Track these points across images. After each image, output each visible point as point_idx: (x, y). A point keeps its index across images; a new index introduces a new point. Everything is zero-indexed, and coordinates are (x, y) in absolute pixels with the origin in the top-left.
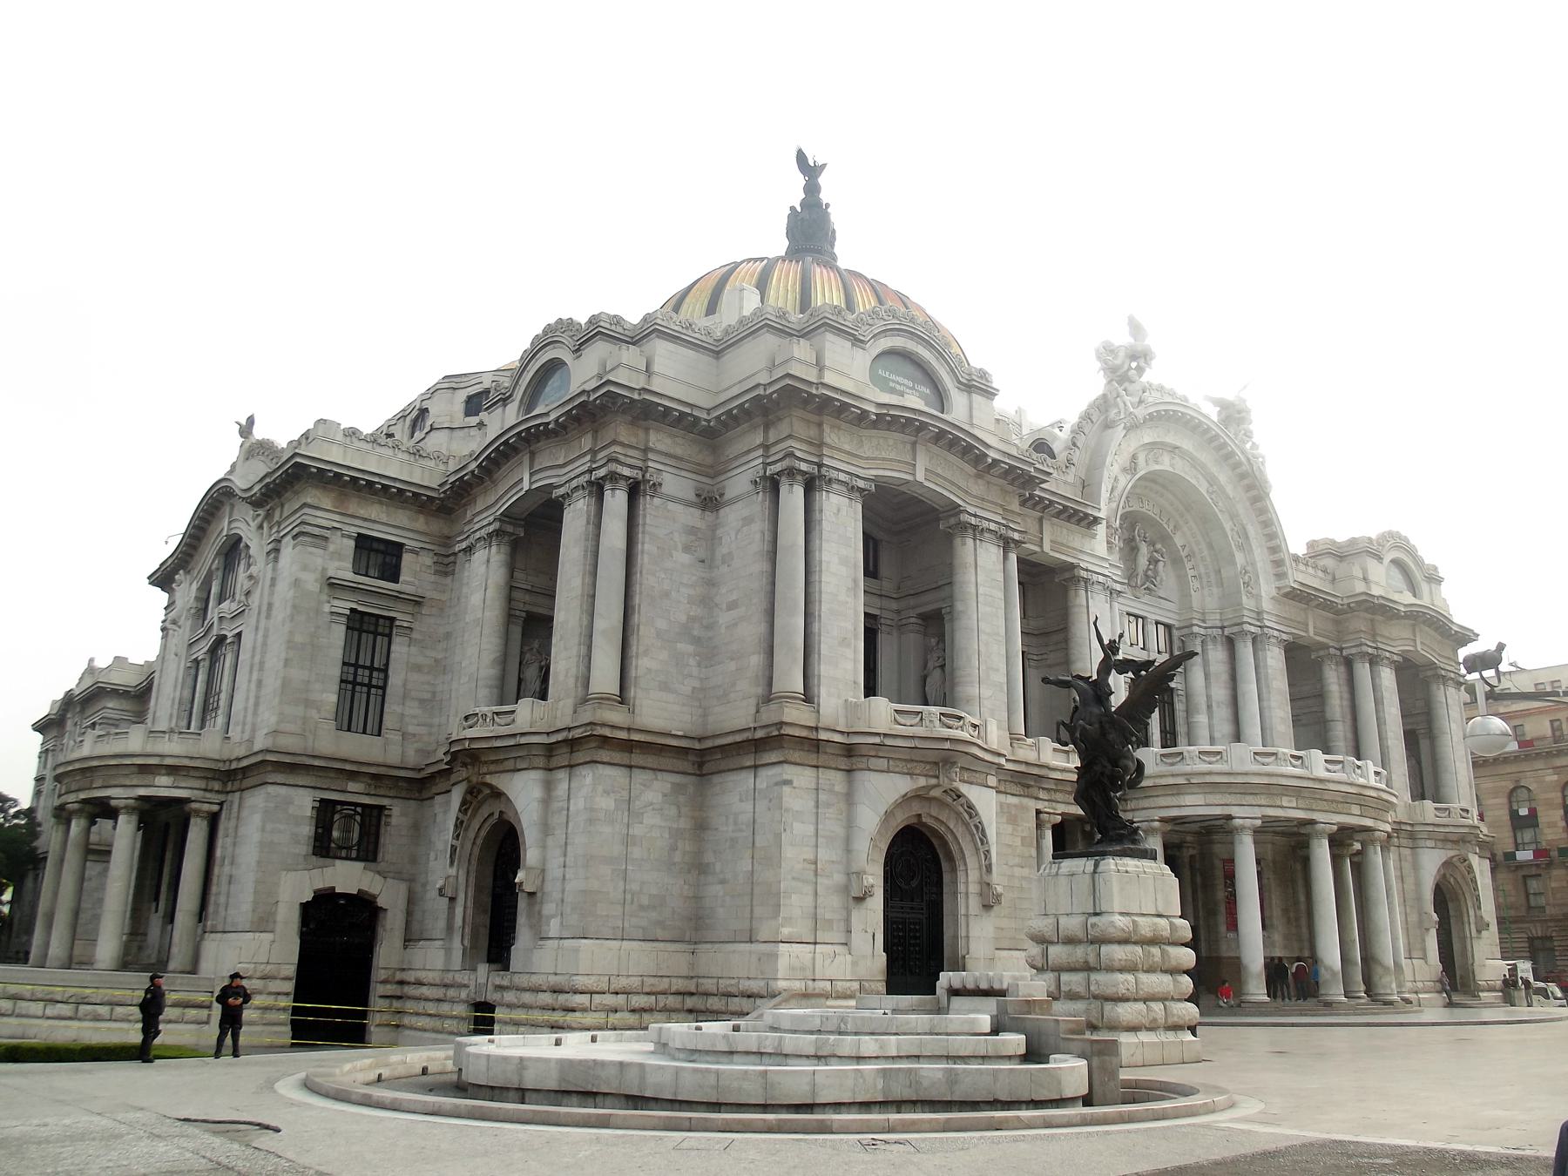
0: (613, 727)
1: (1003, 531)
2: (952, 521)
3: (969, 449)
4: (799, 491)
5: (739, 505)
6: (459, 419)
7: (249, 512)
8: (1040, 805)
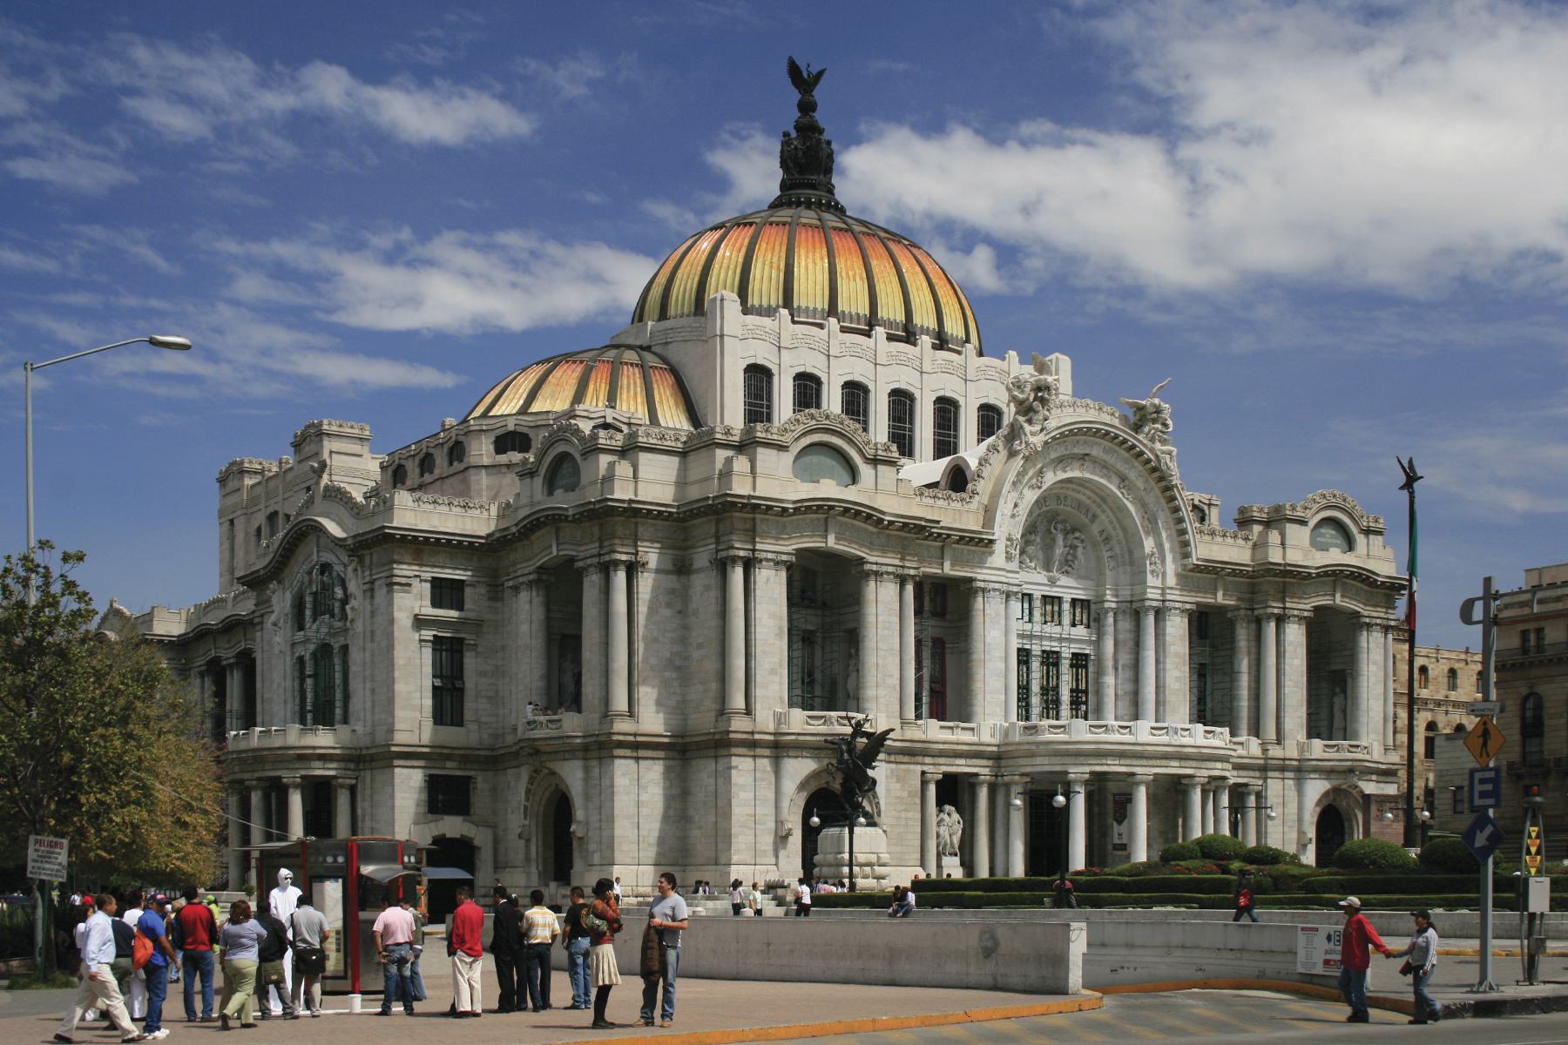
1: (900, 571)
5: (702, 575)
8: (926, 768)
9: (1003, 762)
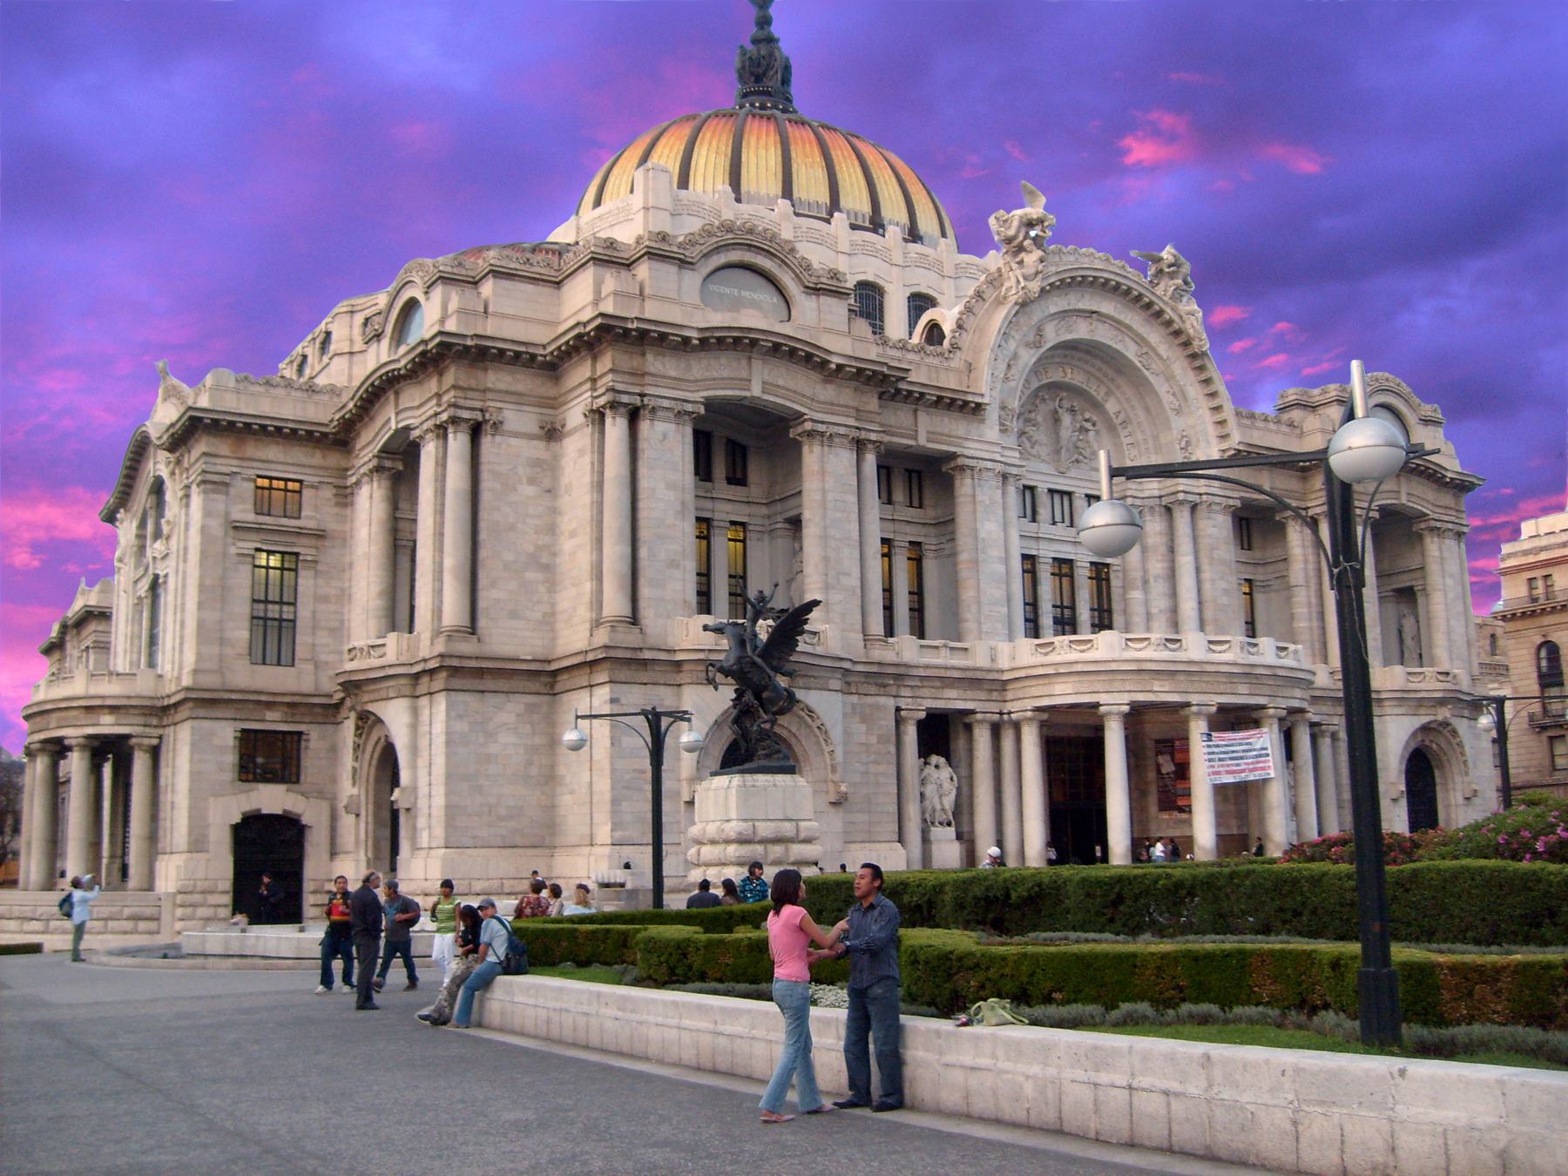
0: (460, 657)
2: (800, 429)
3: (809, 357)
8: (902, 703)
9: (1010, 695)
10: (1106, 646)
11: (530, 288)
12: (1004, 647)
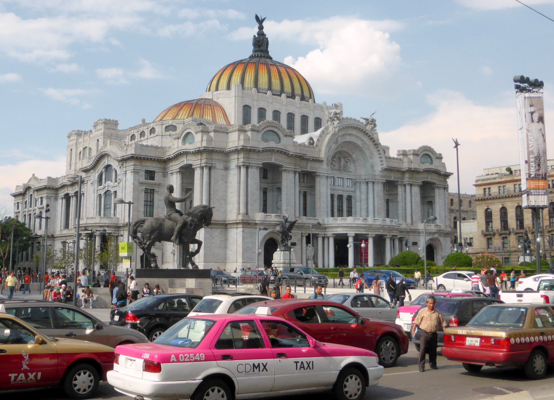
4: (245, 169)
6: (164, 133)
7: (117, 163)
8: (303, 232)
9: (327, 230)
10: (349, 220)
11: (222, 134)
12: (326, 219)
